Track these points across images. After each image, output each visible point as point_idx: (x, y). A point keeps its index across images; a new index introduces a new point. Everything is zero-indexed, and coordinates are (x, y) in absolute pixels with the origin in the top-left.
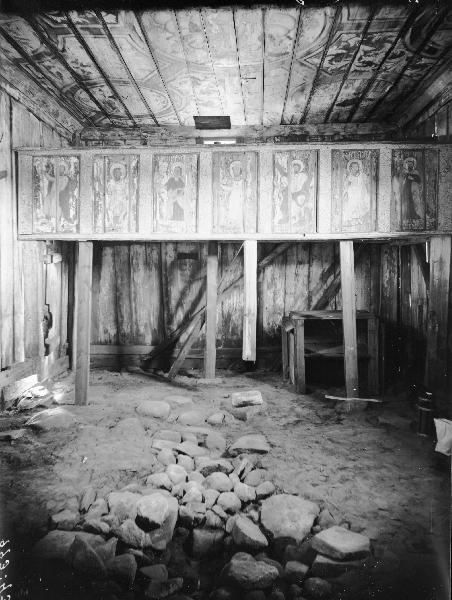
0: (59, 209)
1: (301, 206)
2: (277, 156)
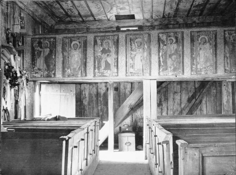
0: (45, 65)
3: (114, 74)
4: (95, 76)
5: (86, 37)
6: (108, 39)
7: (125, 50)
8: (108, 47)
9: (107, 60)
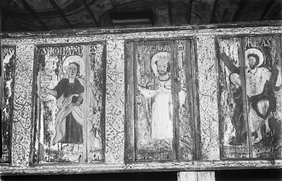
1: (264, 117)
2: (223, 44)
3: (91, 155)
4: (34, 160)
5: (14, 47)
6: (76, 54)
7: (123, 86)
8: (74, 76)
9: (71, 113)
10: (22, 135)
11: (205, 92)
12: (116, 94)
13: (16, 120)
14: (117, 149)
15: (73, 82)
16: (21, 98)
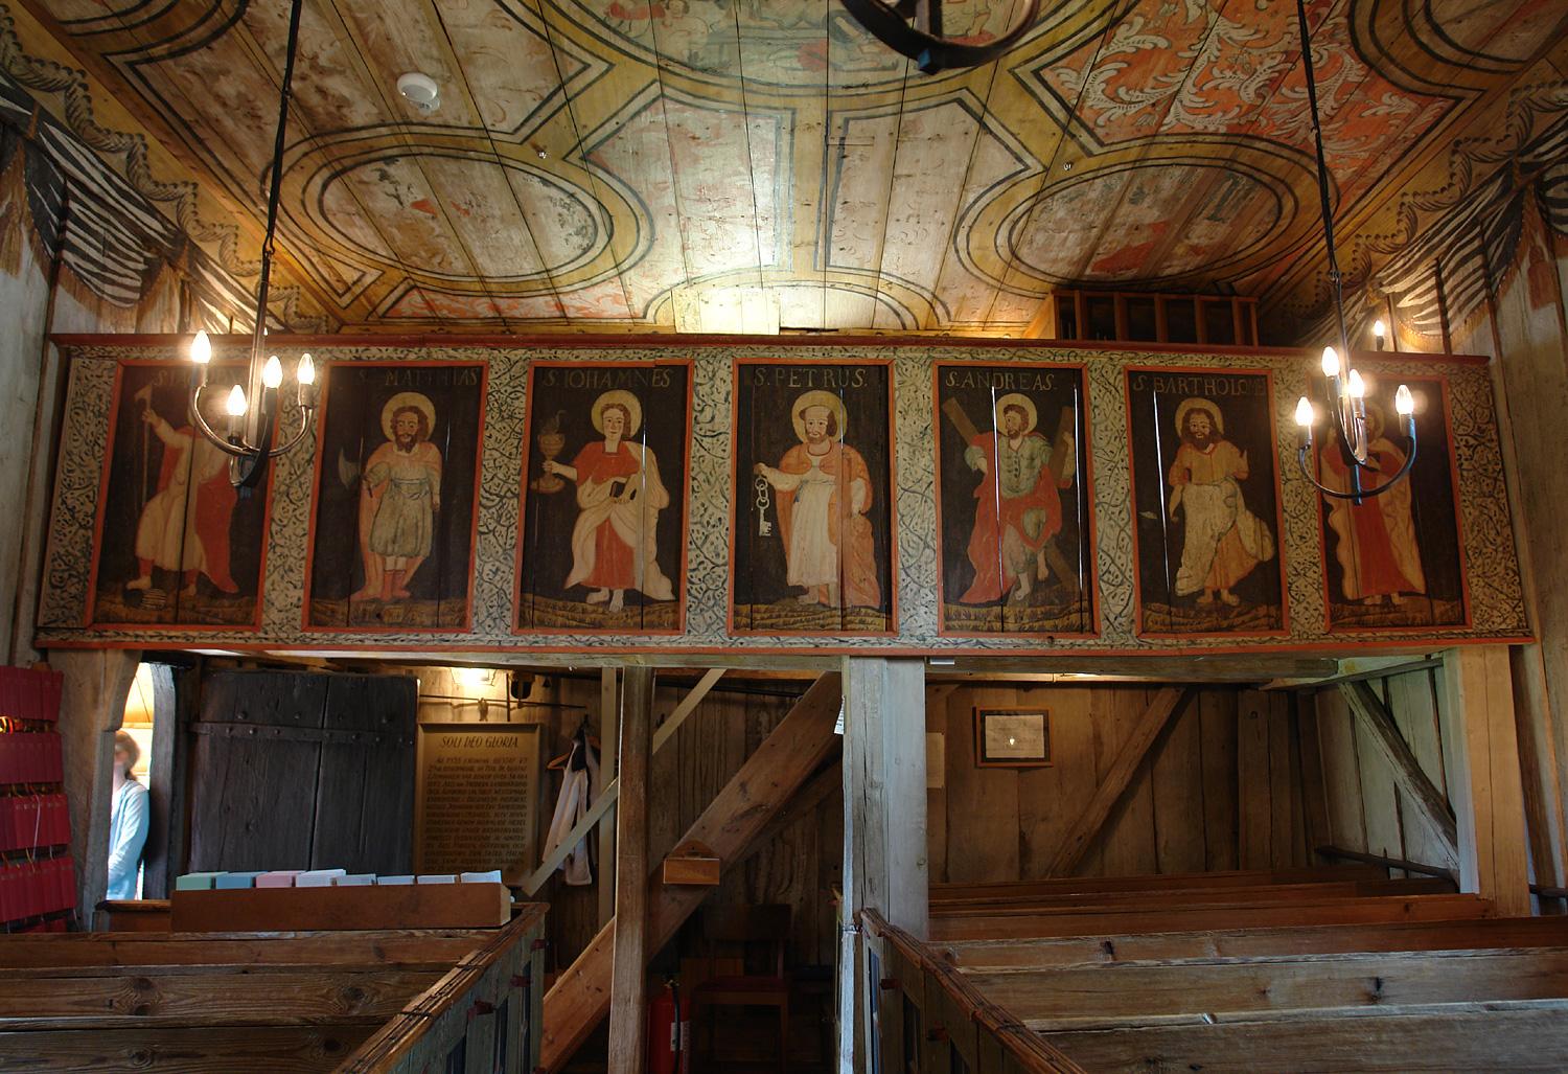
9: (608, 519)
10: (497, 564)
11: (910, 484)
12: (712, 480)
13: (484, 529)
14: (712, 602)
15: (614, 450)
16: (496, 480)
